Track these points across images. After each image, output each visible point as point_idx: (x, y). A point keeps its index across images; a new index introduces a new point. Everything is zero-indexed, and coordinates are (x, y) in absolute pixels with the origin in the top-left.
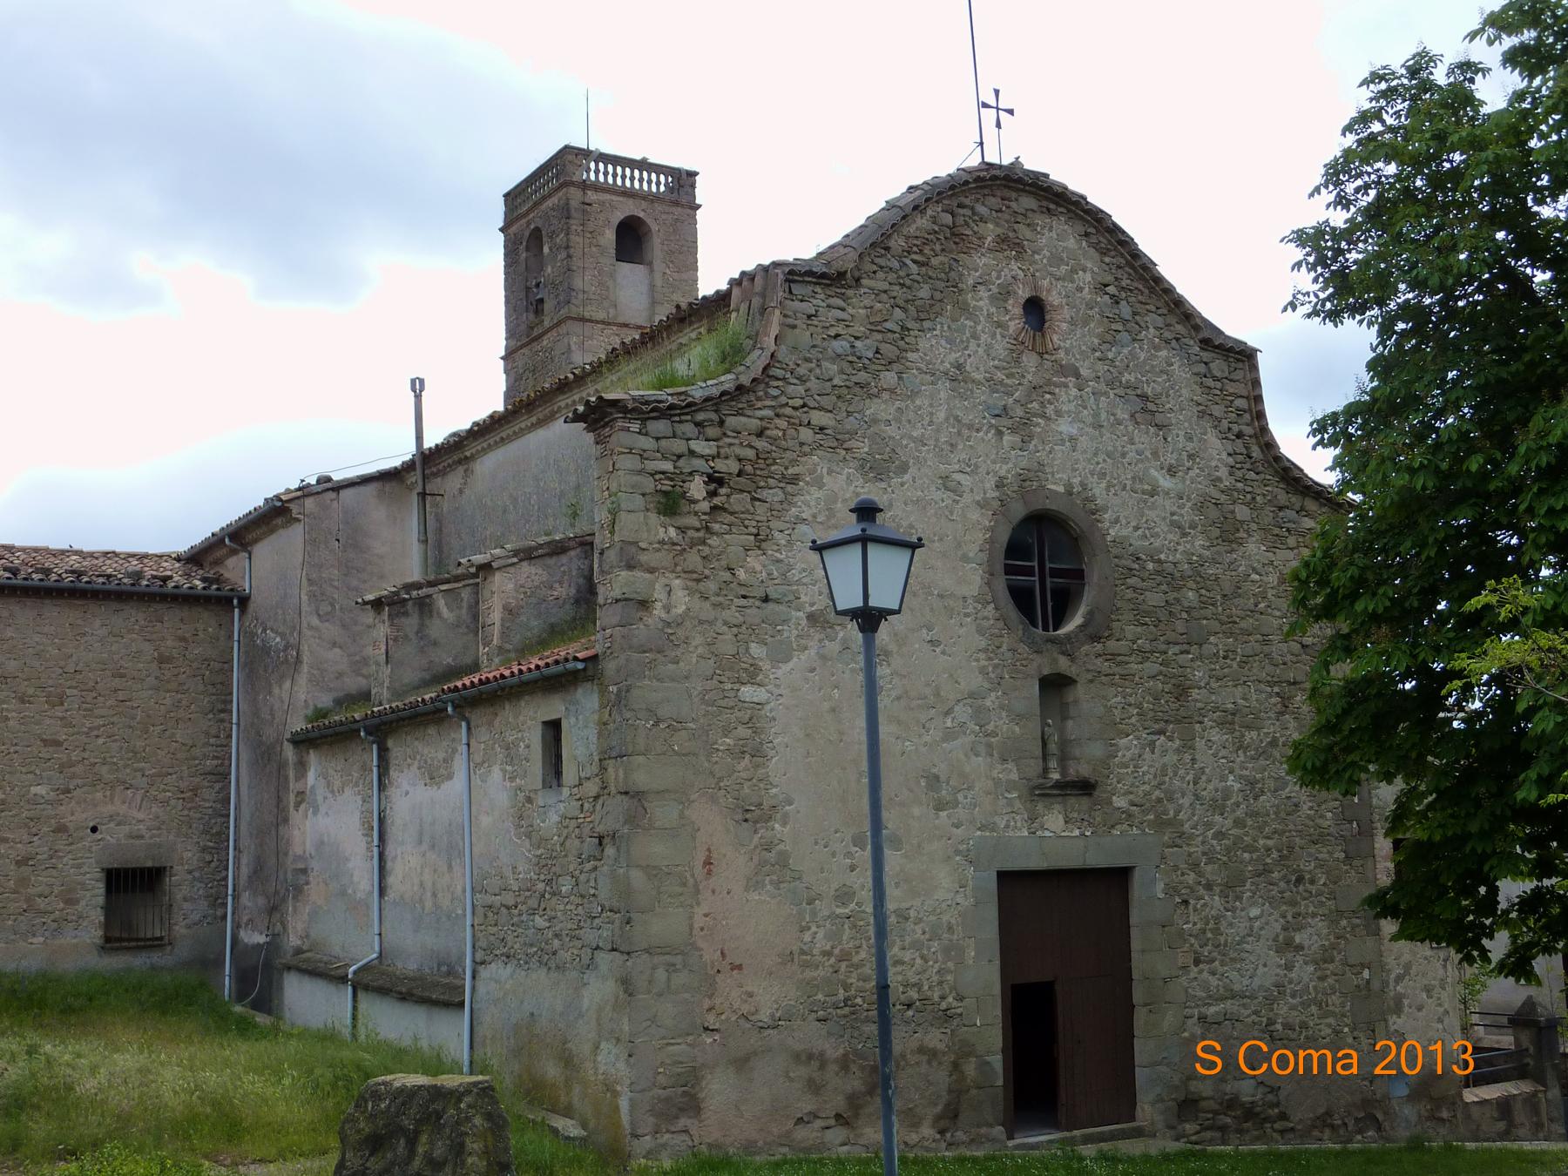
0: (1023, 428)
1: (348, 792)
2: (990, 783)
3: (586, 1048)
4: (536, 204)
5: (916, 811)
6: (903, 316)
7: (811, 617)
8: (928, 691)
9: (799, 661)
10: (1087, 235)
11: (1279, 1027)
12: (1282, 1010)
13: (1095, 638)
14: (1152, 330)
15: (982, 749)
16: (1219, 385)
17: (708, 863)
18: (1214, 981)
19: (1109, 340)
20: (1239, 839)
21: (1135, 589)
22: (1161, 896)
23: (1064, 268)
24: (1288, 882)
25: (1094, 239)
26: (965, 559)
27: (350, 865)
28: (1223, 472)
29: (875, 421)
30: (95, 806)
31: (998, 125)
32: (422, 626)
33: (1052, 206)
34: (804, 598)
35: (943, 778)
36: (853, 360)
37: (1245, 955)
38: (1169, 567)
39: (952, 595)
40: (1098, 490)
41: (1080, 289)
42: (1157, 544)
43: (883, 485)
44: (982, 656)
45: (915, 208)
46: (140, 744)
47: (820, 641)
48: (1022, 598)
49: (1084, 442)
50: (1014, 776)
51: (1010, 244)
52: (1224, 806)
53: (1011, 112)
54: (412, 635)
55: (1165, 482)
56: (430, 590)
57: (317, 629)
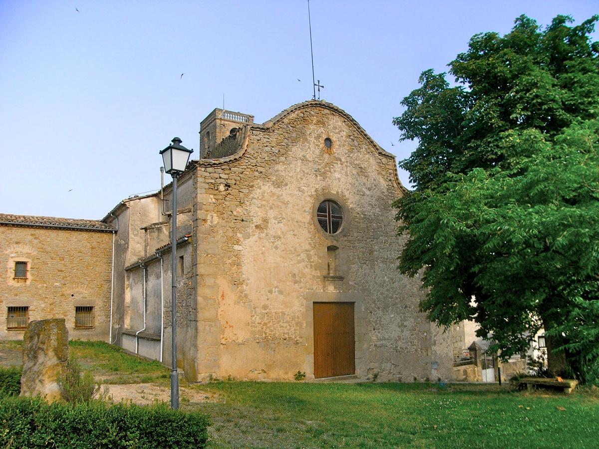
0: (324, 175)
1: (139, 283)
2: (311, 276)
3: (188, 349)
4: (208, 125)
5: (288, 284)
6: (287, 141)
7: (257, 227)
8: (292, 249)
9: (253, 239)
10: (345, 122)
11: (399, 348)
12: (400, 343)
13: (345, 236)
14: (364, 149)
15: (309, 267)
16: (384, 166)
17: (223, 296)
18: (379, 335)
19: (351, 151)
20: (387, 295)
21: (357, 222)
22: (363, 310)
23: (337, 131)
24: (402, 307)
25: (347, 123)
26: (305, 211)
27: (139, 304)
28: (385, 190)
29: (278, 171)
30: (73, 289)
31: (319, 90)
32: (158, 236)
33: (334, 113)
34: (254, 221)
35: (297, 274)
36: (271, 153)
37: (388, 328)
38: (368, 217)
39: (301, 222)
40: (347, 193)
41: (342, 137)
42: (364, 210)
43: (280, 189)
44: (310, 239)
45: (292, 111)
46: (86, 272)
47: (259, 233)
48: (322, 224)
49: (342, 180)
50: (319, 275)
51: (321, 123)
52: (383, 286)
53: (323, 87)
54: (155, 238)
55: (368, 193)
56: (161, 226)
57: (133, 238)
